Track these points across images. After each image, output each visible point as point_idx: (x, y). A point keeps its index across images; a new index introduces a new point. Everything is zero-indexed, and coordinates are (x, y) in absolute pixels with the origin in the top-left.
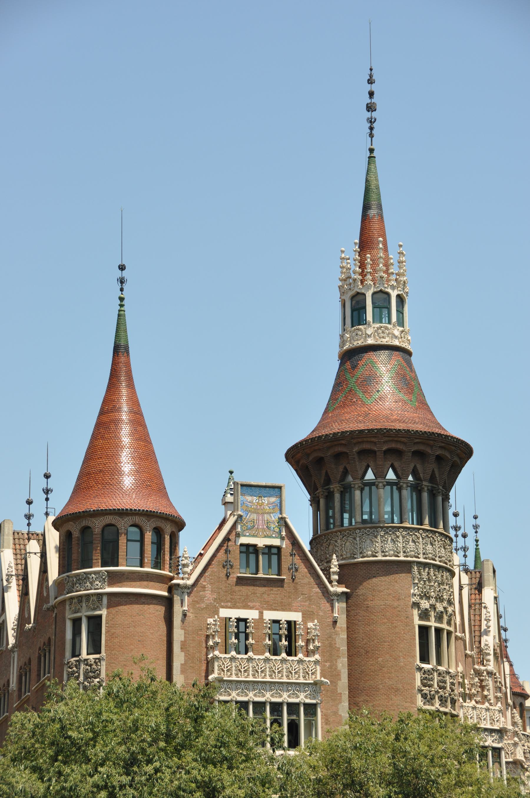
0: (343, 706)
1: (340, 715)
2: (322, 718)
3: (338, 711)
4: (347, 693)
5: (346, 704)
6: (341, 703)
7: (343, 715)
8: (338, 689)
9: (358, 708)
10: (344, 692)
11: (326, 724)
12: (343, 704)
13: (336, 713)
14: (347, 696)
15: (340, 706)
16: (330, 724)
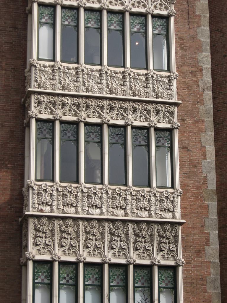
0: (202, 30)
1: (200, 41)
2: (176, 42)
3: (197, 35)
4: (208, 15)
5: (207, 28)
6: (200, 26)
7: (202, 40)
8: (197, 11)
9: (221, 34)
10: (205, 14)
11: (182, 49)
12: (202, 27)
13: (194, 37)
14: (208, 19)
15: (199, 30)
16: (186, 50)
